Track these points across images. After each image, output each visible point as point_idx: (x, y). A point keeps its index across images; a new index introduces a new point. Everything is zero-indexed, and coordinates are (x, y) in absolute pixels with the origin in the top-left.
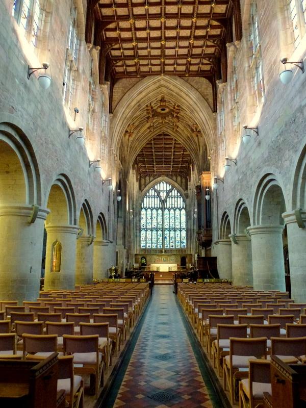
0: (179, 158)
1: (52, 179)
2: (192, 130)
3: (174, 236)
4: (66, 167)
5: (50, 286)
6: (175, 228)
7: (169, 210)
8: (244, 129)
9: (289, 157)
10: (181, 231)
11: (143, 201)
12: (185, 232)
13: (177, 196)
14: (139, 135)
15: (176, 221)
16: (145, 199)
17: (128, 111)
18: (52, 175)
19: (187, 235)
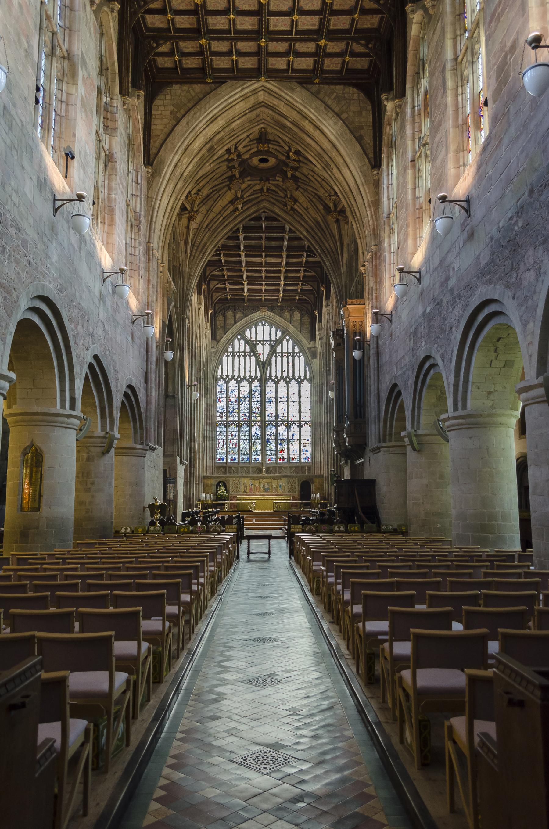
0: (298, 271)
1: (19, 306)
2: (327, 208)
4: (50, 282)
5: (16, 542)
6: (288, 421)
7: (276, 383)
8: (439, 202)
9: (535, 262)
10: (300, 427)
11: (221, 363)
14: (211, 217)
16: (225, 359)
17: (185, 160)
18: (18, 297)
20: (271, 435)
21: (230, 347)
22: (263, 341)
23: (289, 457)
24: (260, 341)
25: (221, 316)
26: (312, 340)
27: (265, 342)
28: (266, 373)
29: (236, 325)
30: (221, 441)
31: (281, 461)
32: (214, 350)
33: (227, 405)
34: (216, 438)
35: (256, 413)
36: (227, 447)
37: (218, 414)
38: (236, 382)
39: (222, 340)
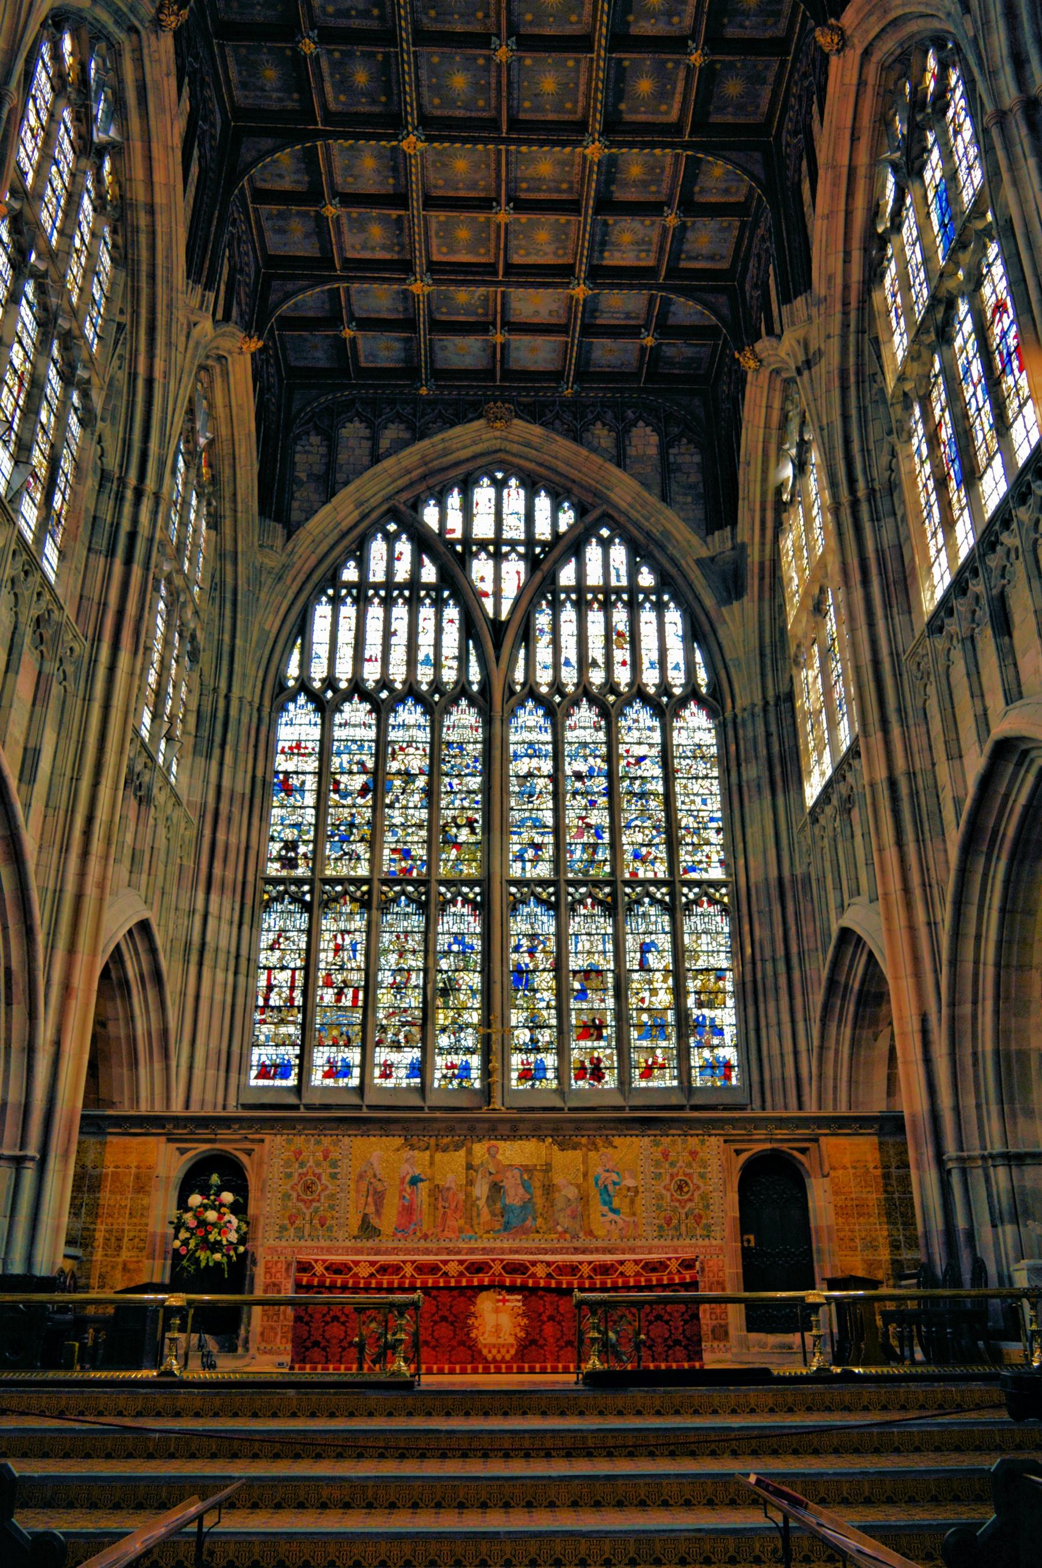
11: (303, 627)
13: (633, 588)
15: (630, 811)
16: (323, 611)
20: (531, 952)
23: (624, 1066)
24: (483, 544)
25: (315, 439)
26: (720, 527)
27: (505, 549)
29: (378, 468)
30: (282, 977)
32: (272, 561)
33: (321, 807)
34: (253, 966)
35: (458, 846)
37: (275, 848)
39: (311, 525)
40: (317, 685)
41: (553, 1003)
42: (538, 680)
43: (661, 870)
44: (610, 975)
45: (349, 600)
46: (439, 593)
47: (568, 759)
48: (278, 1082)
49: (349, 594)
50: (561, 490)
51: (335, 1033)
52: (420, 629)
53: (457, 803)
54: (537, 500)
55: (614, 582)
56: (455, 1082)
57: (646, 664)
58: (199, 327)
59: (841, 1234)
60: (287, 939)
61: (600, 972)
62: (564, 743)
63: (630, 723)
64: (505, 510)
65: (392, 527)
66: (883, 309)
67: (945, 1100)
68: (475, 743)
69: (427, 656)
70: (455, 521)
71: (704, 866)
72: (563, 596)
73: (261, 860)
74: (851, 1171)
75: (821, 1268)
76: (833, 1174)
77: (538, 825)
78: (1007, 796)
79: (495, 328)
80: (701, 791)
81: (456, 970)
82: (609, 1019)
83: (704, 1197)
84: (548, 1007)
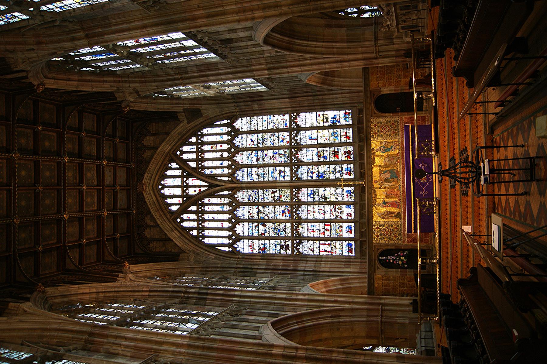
3: (315, 150)
6: (290, 148)
7: (238, 167)
10: (299, 129)
11: (213, 246)
12: (303, 115)
15: (269, 144)
16: (206, 241)
19: (310, 109)
20: (313, 173)
21: (191, 232)
22: (182, 187)
24: (183, 191)
25: (151, 245)
26: (177, 117)
27: (185, 184)
28: (224, 181)
29: (160, 225)
30: (322, 248)
31: (352, 156)
32: (192, 257)
33: (270, 238)
34: (319, 256)
35: (280, 196)
36: (331, 239)
37: (282, 252)
38: (237, 226)
40: (231, 241)
41: (328, 166)
42: (227, 173)
43: (286, 134)
44: (319, 149)
45: (203, 233)
46: (200, 204)
47: (253, 163)
48: (353, 247)
49: (201, 233)
50: (165, 167)
51: (338, 231)
52: (212, 210)
53: (267, 197)
54: (168, 175)
55: (195, 150)
56: (352, 194)
57: (221, 139)
58: (131, 278)
59: (396, 84)
60: (310, 246)
61: (318, 152)
62: (247, 165)
63: (240, 144)
64: (172, 184)
65: (179, 220)
66: (123, 71)
67: (360, 56)
68: (248, 192)
69: (220, 208)
70: (176, 200)
71: (285, 121)
72: (200, 166)
73: (286, 255)
74: (379, 81)
75: (405, 90)
76: (380, 87)
77: (273, 172)
78: (278, 40)
79: (115, 189)
80: (261, 122)
81: (319, 195)
82: (332, 149)
83: (387, 123)
84: (329, 167)
